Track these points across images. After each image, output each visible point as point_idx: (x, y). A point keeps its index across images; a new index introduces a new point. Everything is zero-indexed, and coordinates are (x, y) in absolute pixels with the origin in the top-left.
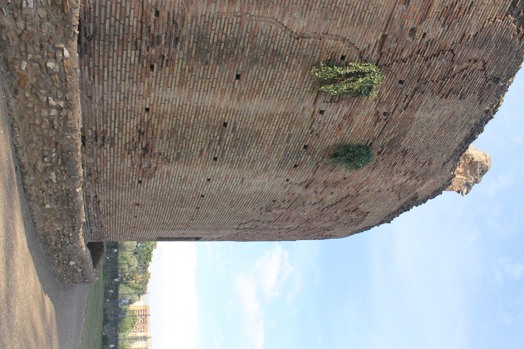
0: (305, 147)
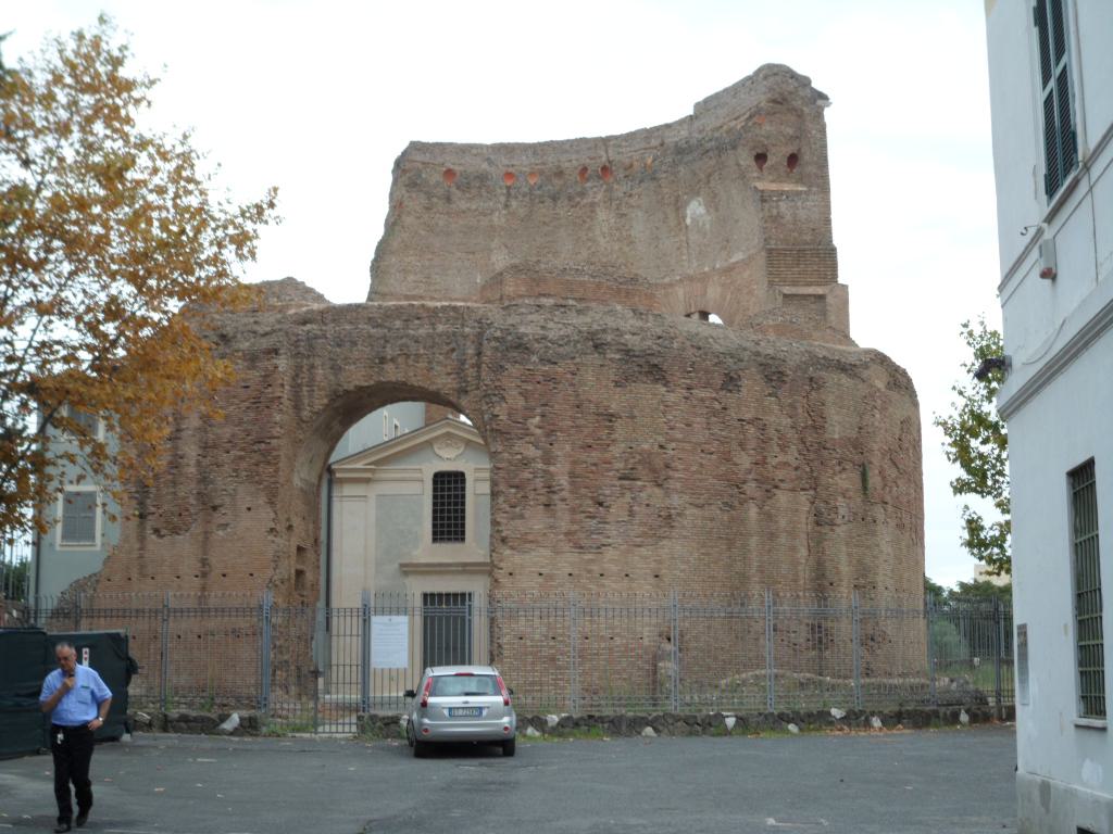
0: (863, 519)
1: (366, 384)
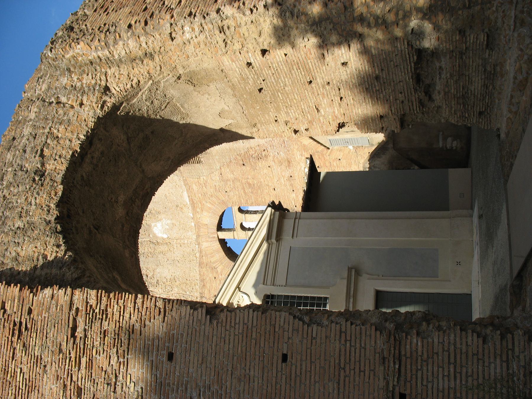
1: (60, 193)
